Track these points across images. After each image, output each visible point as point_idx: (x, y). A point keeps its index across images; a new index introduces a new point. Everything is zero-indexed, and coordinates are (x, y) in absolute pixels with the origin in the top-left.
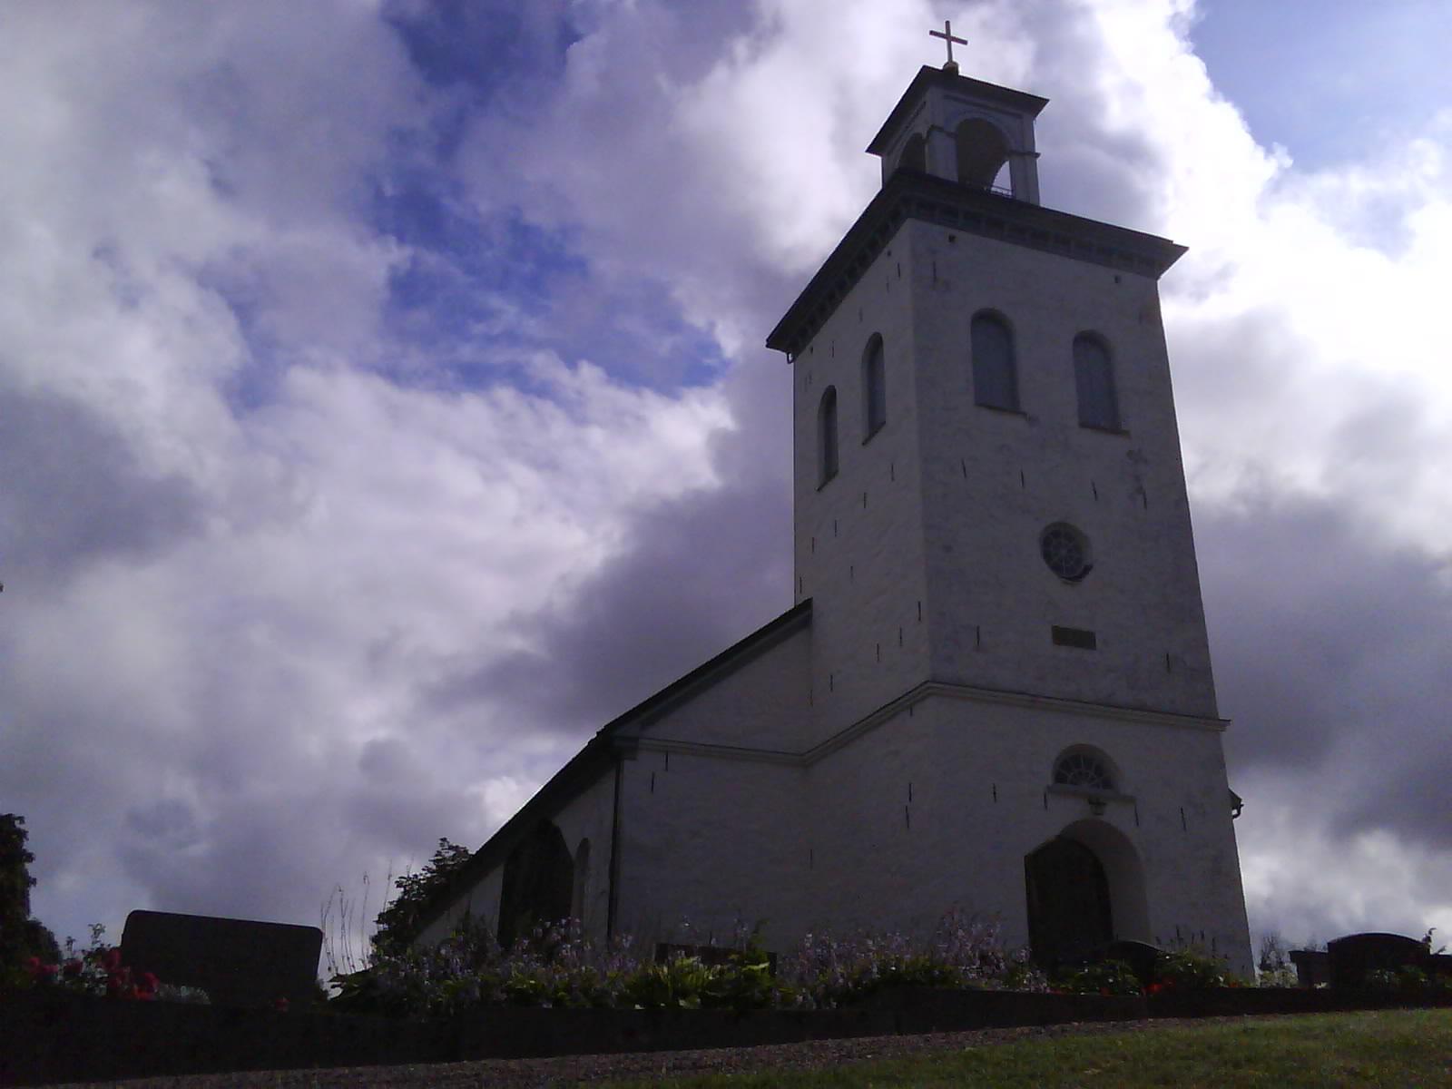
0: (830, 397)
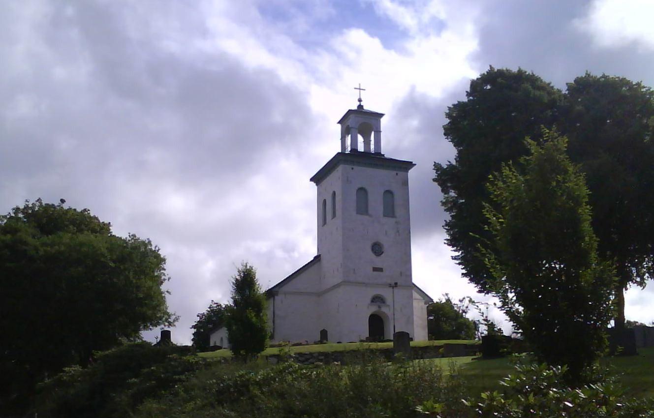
0: (325, 201)
